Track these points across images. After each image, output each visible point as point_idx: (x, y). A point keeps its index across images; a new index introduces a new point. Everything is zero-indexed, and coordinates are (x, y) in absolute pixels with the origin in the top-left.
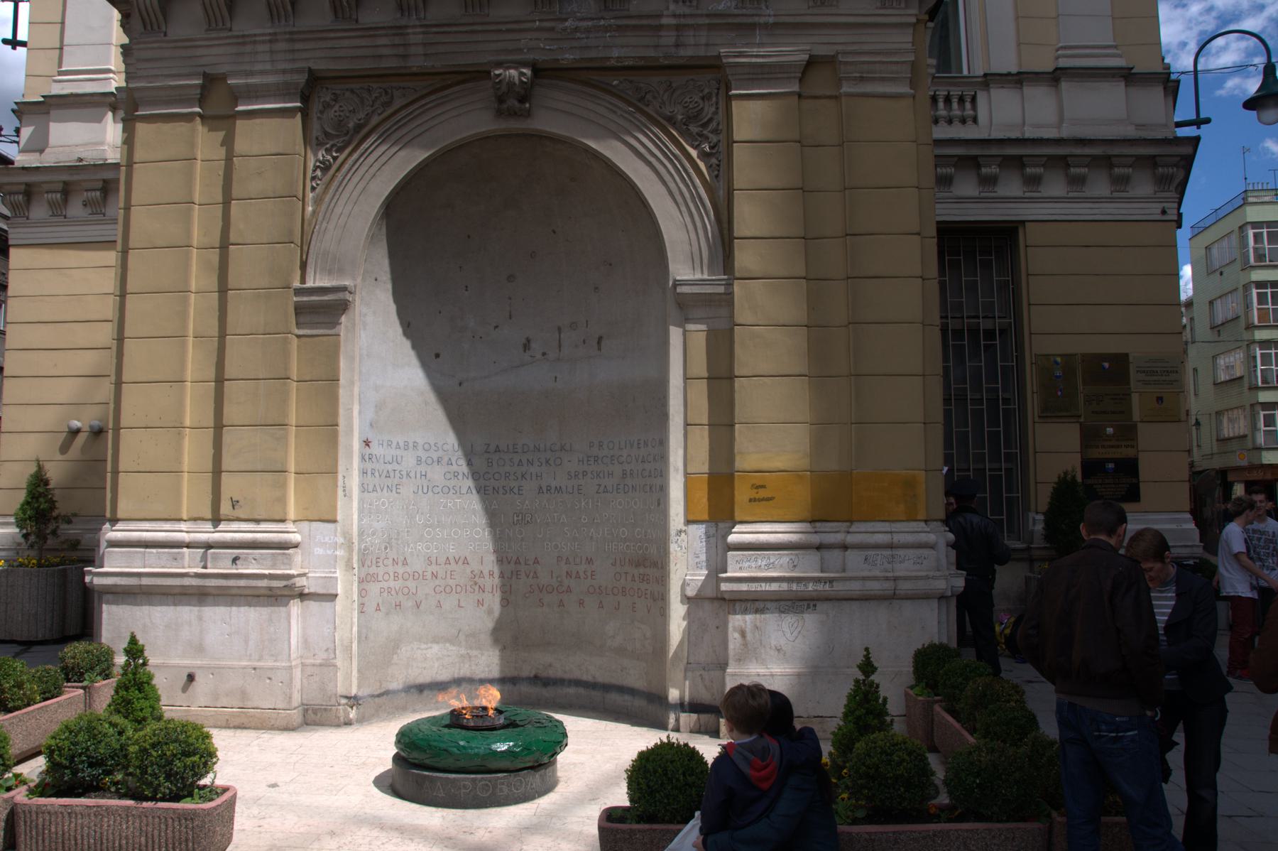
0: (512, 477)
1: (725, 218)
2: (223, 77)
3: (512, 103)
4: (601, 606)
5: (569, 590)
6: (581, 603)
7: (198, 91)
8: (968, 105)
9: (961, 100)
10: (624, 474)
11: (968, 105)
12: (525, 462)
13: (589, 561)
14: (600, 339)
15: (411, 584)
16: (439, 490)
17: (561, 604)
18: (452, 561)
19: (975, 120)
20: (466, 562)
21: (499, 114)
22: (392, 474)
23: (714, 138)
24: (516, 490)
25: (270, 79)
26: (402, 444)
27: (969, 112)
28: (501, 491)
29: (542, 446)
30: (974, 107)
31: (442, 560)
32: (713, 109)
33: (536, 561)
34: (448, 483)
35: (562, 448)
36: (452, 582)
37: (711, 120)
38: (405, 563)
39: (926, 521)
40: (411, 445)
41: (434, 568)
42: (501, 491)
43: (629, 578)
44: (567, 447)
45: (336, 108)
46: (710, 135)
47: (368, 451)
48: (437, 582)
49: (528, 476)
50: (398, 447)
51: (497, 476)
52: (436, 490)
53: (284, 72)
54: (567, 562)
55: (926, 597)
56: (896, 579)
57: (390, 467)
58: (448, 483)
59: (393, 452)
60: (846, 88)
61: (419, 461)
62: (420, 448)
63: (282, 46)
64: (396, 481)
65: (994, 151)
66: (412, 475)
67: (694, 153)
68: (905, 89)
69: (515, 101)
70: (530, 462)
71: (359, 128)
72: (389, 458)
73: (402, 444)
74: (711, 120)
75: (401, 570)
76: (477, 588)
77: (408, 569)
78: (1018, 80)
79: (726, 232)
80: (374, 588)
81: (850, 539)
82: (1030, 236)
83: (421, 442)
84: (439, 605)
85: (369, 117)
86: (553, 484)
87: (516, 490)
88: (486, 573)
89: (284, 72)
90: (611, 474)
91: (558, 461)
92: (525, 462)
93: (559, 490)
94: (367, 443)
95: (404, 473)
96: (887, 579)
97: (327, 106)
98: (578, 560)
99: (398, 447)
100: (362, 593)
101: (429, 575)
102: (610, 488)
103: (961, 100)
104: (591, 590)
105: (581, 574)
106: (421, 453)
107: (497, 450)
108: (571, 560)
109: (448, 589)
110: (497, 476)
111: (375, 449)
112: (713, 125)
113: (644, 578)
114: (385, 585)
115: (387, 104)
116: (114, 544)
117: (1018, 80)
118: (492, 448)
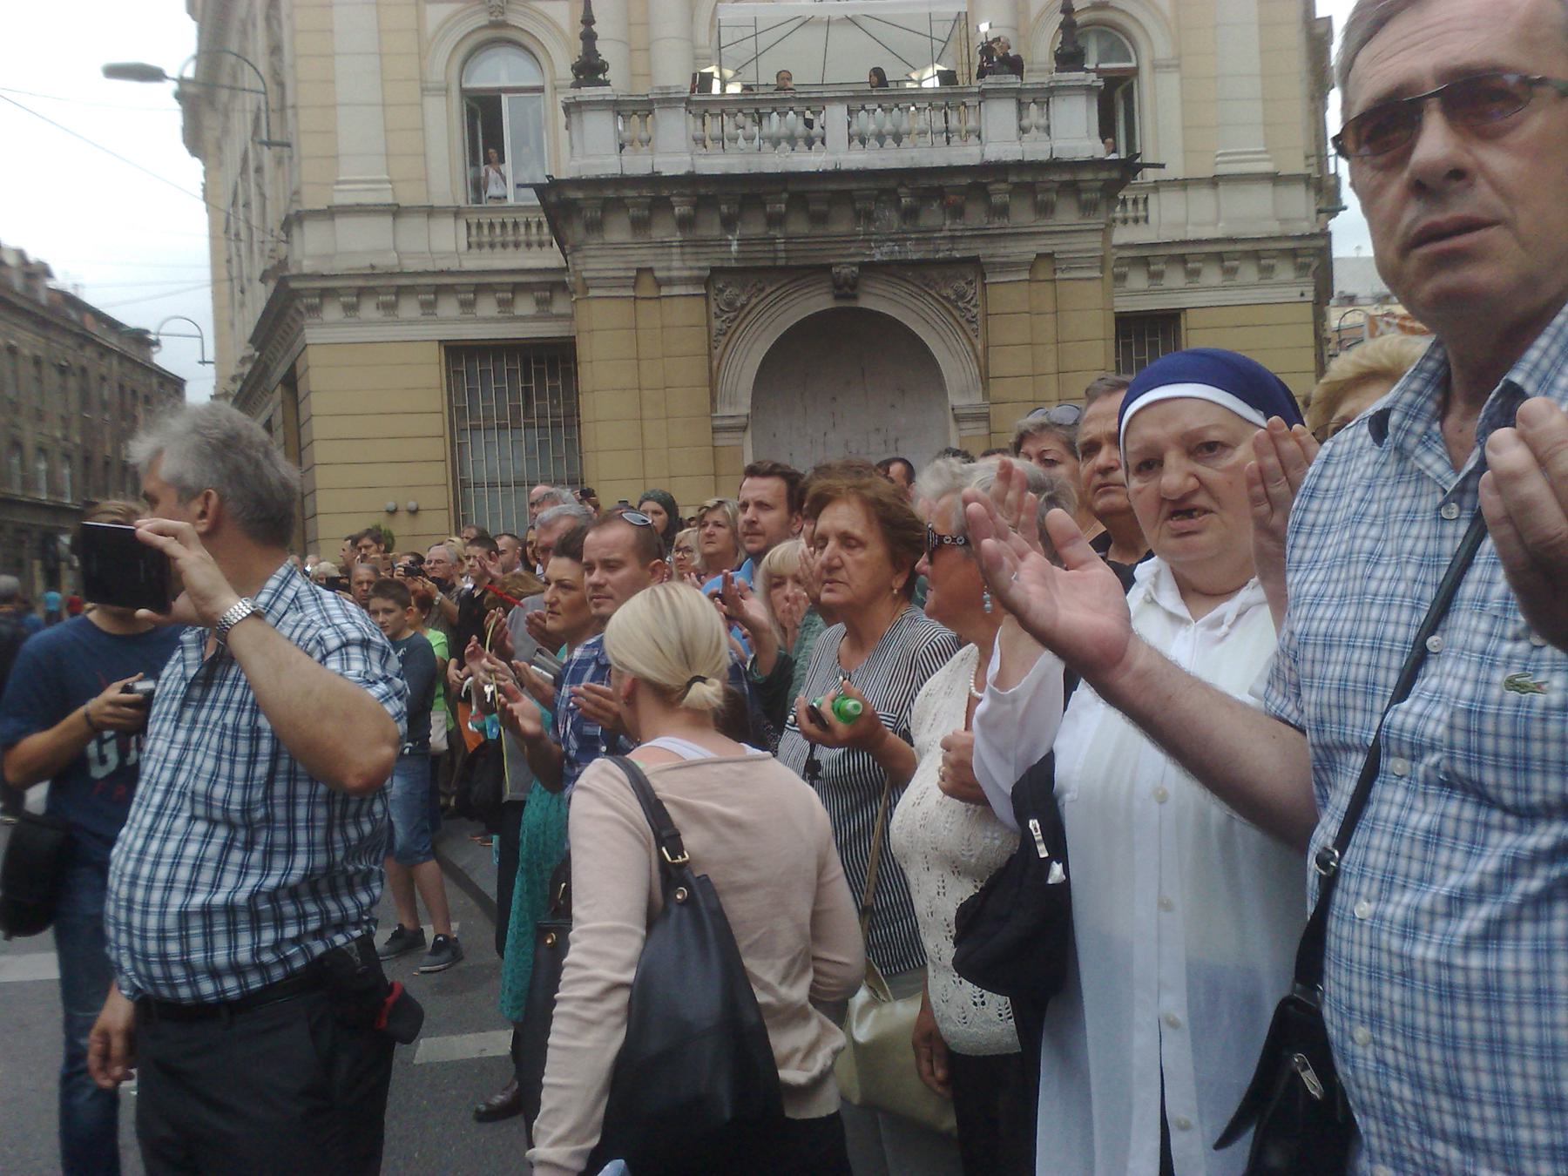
2: (651, 270)
3: (846, 289)
8: (1141, 206)
9: (1135, 202)
11: (1141, 206)
14: (897, 440)
19: (1146, 220)
21: (837, 297)
23: (975, 311)
25: (686, 273)
27: (1141, 213)
30: (1146, 209)
53: (691, 268)
60: (1059, 275)
63: (688, 250)
65: (1161, 252)
67: (963, 321)
68: (1096, 274)
69: (846, 289)
71: (743, 306)
78: (1184, 184)
82: (1188, 321)
85: (749, 299)
89: (691, 268)
97: (721, 291)
103: (1135, 202)
115: (762, 290)
117: (1184, 184)
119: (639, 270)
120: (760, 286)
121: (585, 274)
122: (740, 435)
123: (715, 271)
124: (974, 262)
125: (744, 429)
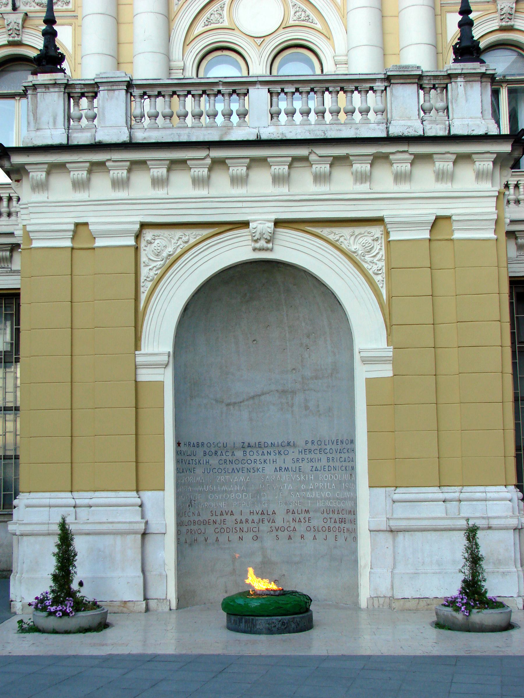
0: (258, 462)
1: (387, 312)
2: (86, 224)
4: (315, 538)
5: (294, 530)
6: (302, 537)
7: (71, 233)
10: (328, 460)
12: (266, 453)
13: (307, 511)
15: (202, 527)
16: (216, 470)
17: (290, 538)
18: (224, 513)
20: (232, 514)
22: (191, 463)
24: (261, 470)
26: (196, 444)
28: (252, 471)
29: (276, 443)
31: (218, 513)
32: (379, 247)
33: (274, 513)
34: (221, 466)
35: (289, 444)
36: (225, 527)
37: (378, 253)
38: (199, 515)
39: (505, 486)
40: (200, 444)
41: (214, 518)
42: (252, 471)
43: (333, 521)
44: (292, 444)
45: (155, 244)
46: (378, 262)
47: (179, 449)
48: (217, 525)
49: (268, 461)
50: (194, 446)
51: (249, 462)
52: (215, 471)
54: (293, 512)
55: (505, 528)
56: (488, 518)
57: (190, 458)
58: (221, 466)
59: (192, 449)
60: (457, 235)
61: (205, 454)
62: (205, 446)
64: (194, 466)
66: (201, 462)
70: (269, 453)
72: (189, 453)
73: (196, 444)
74: (378, 253)
75: (196, 519)
76: (238, 529)
77: (201, 518)
79: (388, 320)
80: (184, 529)
81: (463, 496)
83: (206, 443)
84: (217, 540)
86: (283, 466)
87: (261, 470)
88: (244, 520)
90: (319, 460)
91: (286, 452)
92: (266, 453)
93: (287, 469)
94: (179, 444)
95: (197, 461)
96: (483, 518)
98: (300, 512)
99: (194, 446)
100: (178, 533)
101: (211, 521)
102: (319, 468)
104: (309, 529)
105: (303, 520)
106: (205, 448)
107: (249, 446)
108: (296, 511)
109: (222, 530)
110: (249, 462)
111: (183, 448)
112: (379, 256)
113: (342, 521)
114: (189, 528)
116: (27, 506)
118: (246, 445)
119: (77, 225)
120: (185, 239)
121: (29, 228)
122: (161, 371)
123: (144, 225)
124: (378, 221)
125: (167, 365)
